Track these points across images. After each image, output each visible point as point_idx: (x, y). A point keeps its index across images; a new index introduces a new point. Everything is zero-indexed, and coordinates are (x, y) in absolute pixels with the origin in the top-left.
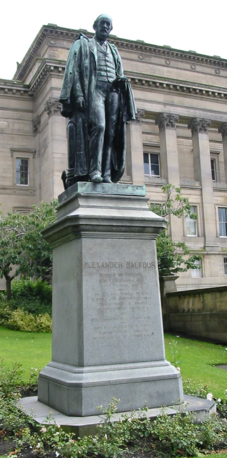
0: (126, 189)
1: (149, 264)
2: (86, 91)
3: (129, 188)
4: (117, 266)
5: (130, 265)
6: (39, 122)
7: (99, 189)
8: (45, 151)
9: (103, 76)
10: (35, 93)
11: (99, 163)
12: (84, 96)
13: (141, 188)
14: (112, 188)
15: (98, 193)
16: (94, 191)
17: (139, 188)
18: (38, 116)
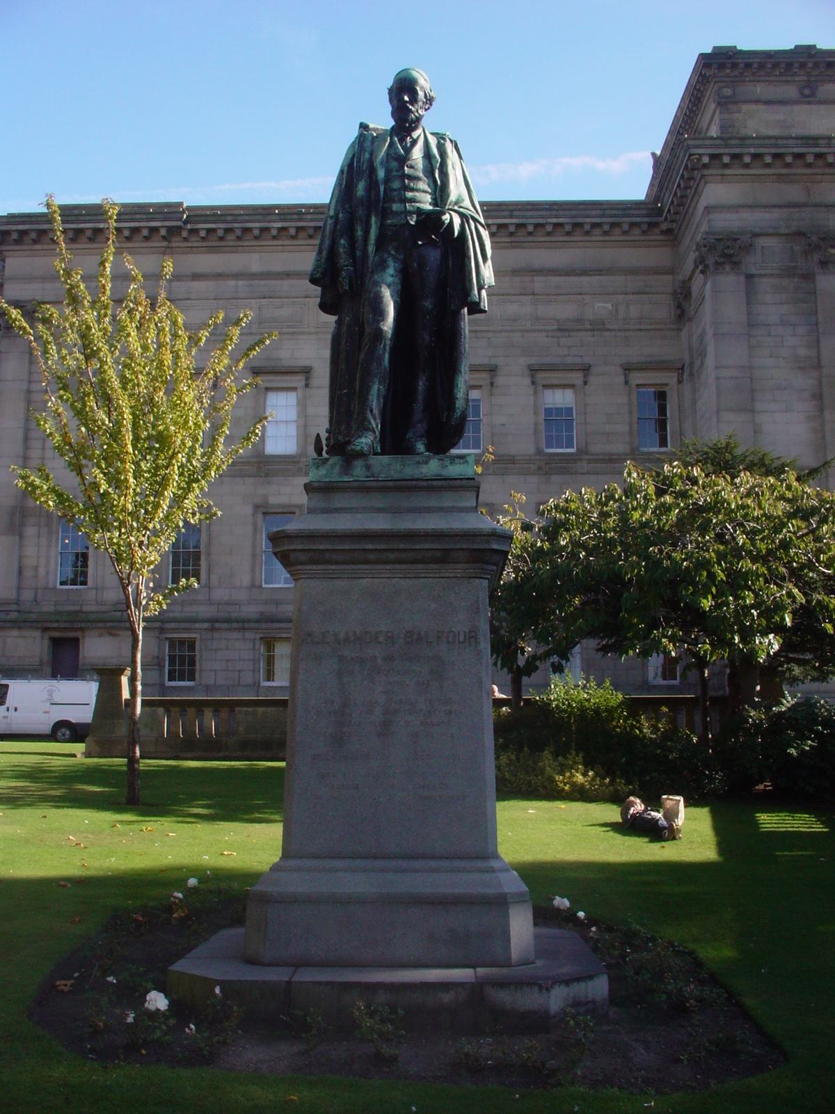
1: (462, 633)
3: (431, 462)
4: (381, 639)
5: (414, 638)
6: (687, 295)
7: (359, 469)
8: (702, 363)
10: (674, 224)
13: (462, 461)
16: (347, 474)
17: (457, 461)
18: (684, 282)
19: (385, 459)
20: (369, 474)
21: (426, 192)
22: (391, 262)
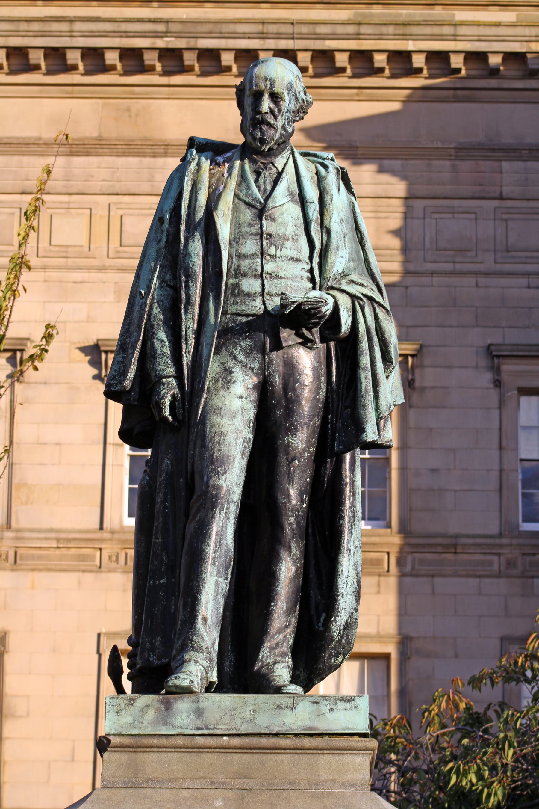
0: (289, 712)
2: (186, 359)
7: (184, 716)
9: (248, 295)
11: (205, 620)
12: (179, 376)
13: (348, 705)
14: (235, 709)
15: (180, 731)
16: (166, 724)
17: (341, 705)
19: (228, 700)
20: (199, 724)
21: (297, 260)
22: (238, 373)
